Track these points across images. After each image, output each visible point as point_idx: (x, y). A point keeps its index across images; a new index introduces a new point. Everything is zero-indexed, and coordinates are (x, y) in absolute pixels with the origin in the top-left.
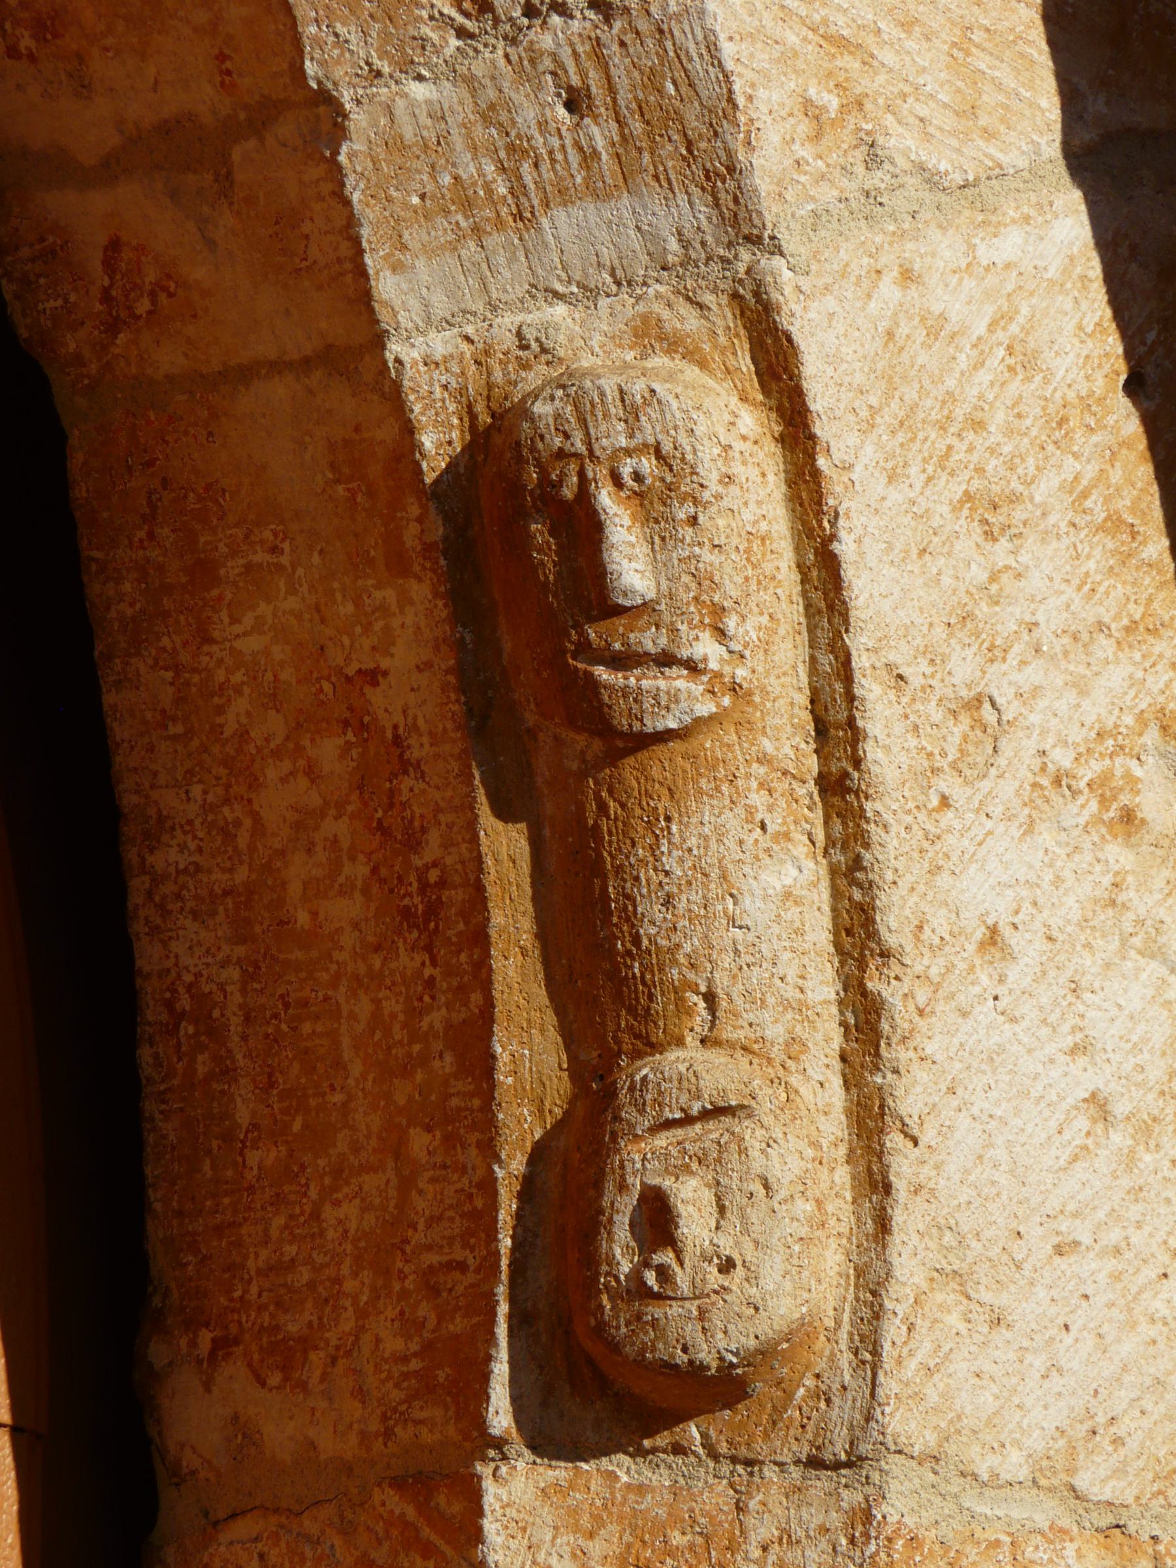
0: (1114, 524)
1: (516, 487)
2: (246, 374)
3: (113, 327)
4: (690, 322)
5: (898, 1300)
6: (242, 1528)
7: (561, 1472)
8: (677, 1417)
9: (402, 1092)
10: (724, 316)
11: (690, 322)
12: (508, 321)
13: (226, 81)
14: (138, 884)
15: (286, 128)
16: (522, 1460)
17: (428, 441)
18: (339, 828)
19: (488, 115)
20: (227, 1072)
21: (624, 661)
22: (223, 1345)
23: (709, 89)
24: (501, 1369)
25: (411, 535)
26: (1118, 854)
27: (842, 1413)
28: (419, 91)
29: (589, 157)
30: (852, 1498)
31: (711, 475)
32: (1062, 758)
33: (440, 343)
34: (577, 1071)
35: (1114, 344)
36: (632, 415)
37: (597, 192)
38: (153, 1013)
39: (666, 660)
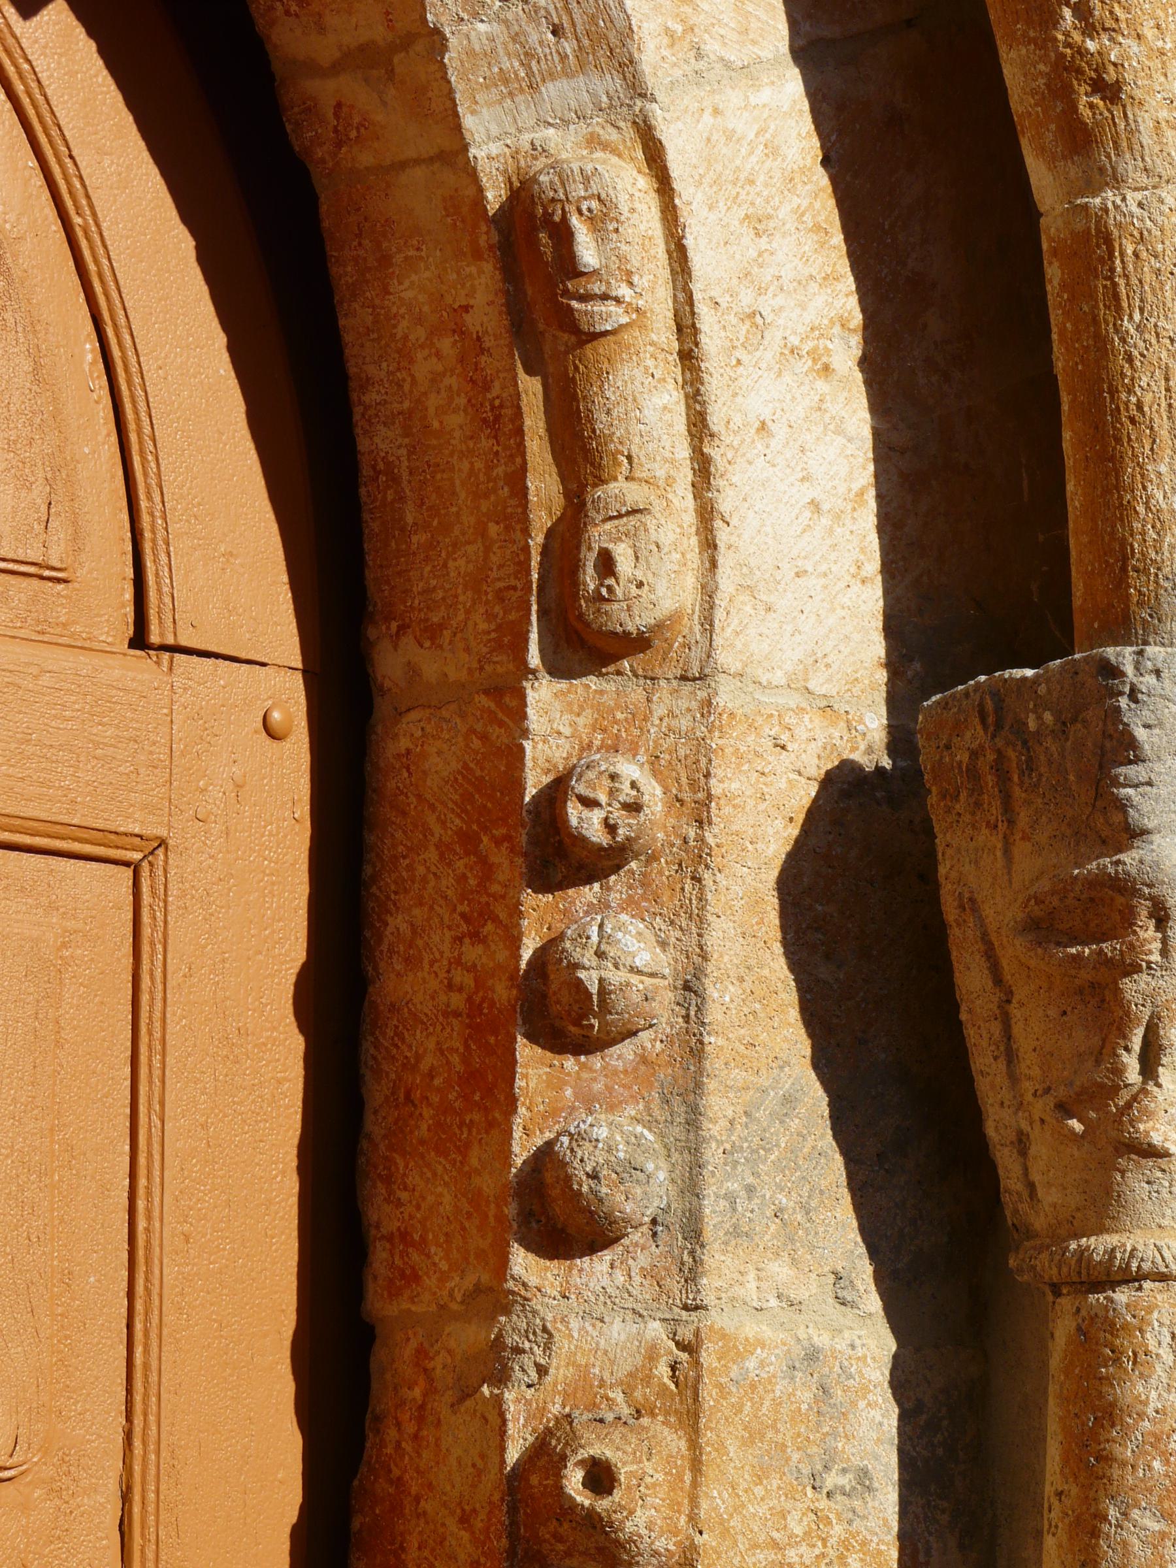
0: (817, 228)
1: (532, 216)
2: (403, 165)
3: (339, 145)
4: (612, 135)
5: (721, 600)
6: (414, 715)
7: (563, 685)
8: (616, 658)
9: (485, 506)
10: (629, 133)
11: (612, 135)
12: (527, 137)
13: (390, 24)
14: (358, 411)
15: (419, 47)
16: (545, 679)
17: (490, 195)
18: (452, 381)
19: (515, 38)
20: (402, 499)
21: (585, 298)
22: (402, 628)
23: (620, 23)
24: (534, 636)
25: (483, 241)
26: (822, 386)
27: (696, 654)
28: (482, 27)
29: (563, 57)
30: (703, 695)
31: (624, 209)
32: (794, 341)
33: (495, 148)
34: (567, 494)
35: (816, 142)
36: (586, 181)
37: (568, 74)
38: (366, 471)
39: (605, 297)
